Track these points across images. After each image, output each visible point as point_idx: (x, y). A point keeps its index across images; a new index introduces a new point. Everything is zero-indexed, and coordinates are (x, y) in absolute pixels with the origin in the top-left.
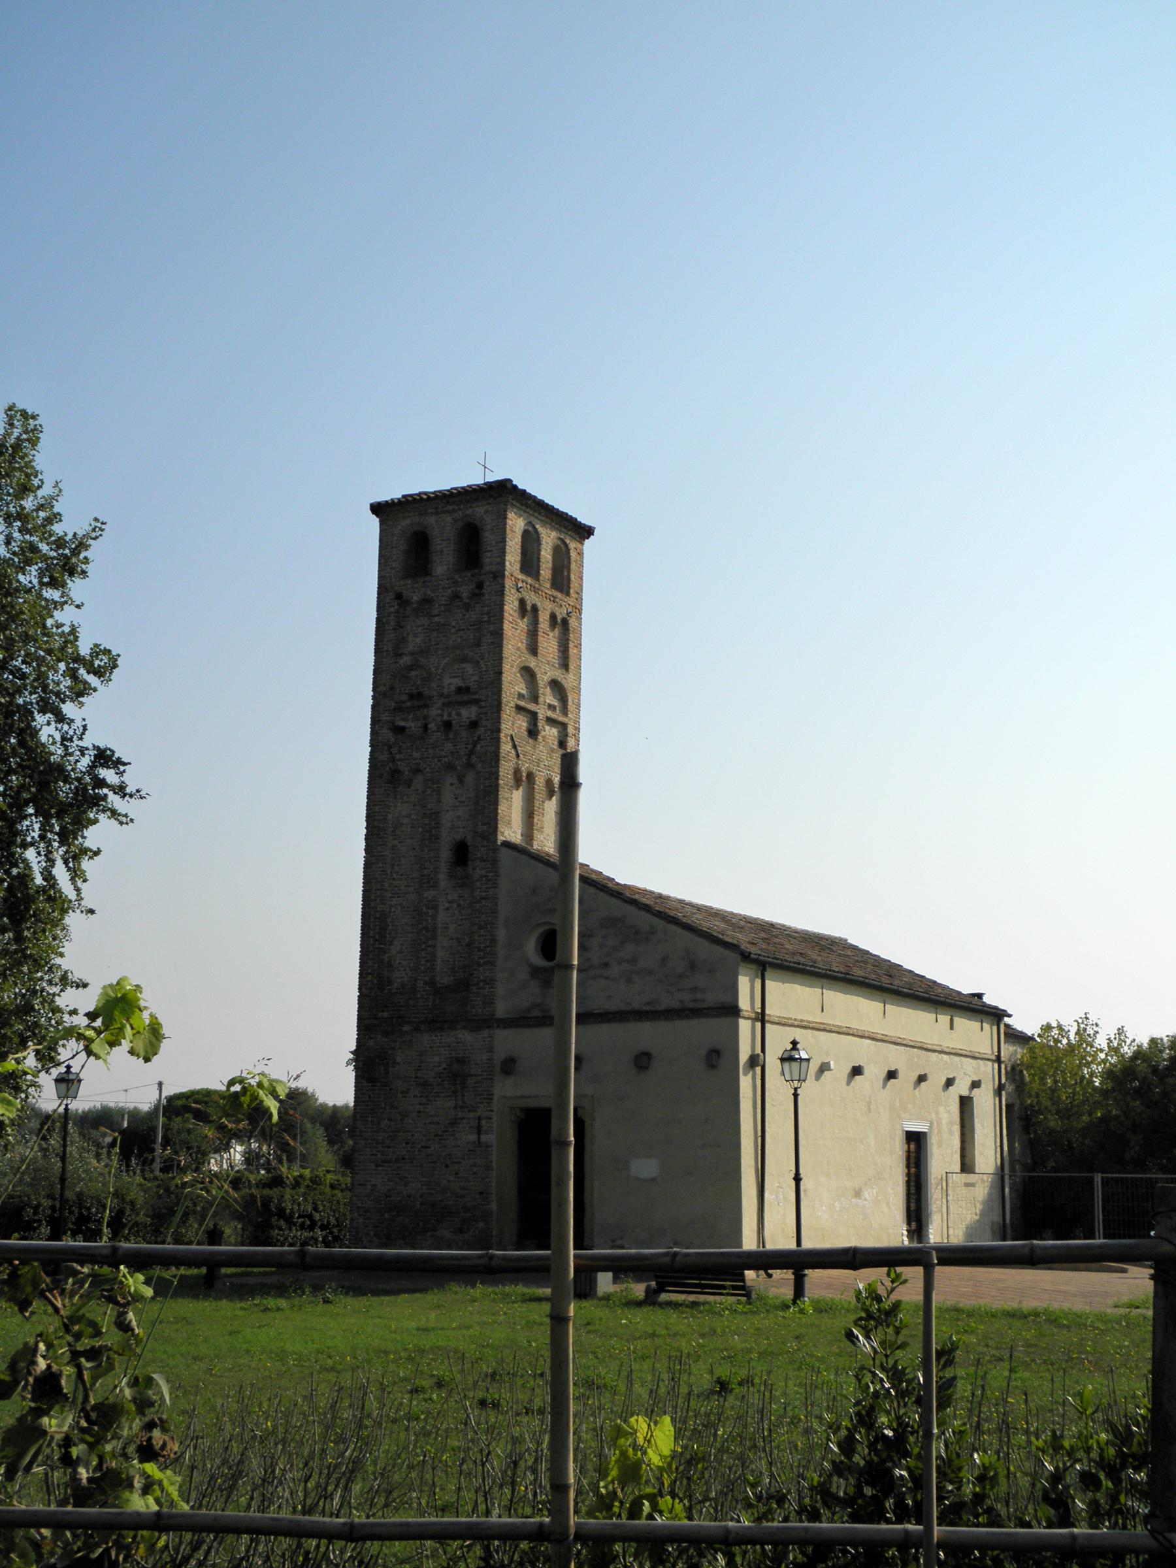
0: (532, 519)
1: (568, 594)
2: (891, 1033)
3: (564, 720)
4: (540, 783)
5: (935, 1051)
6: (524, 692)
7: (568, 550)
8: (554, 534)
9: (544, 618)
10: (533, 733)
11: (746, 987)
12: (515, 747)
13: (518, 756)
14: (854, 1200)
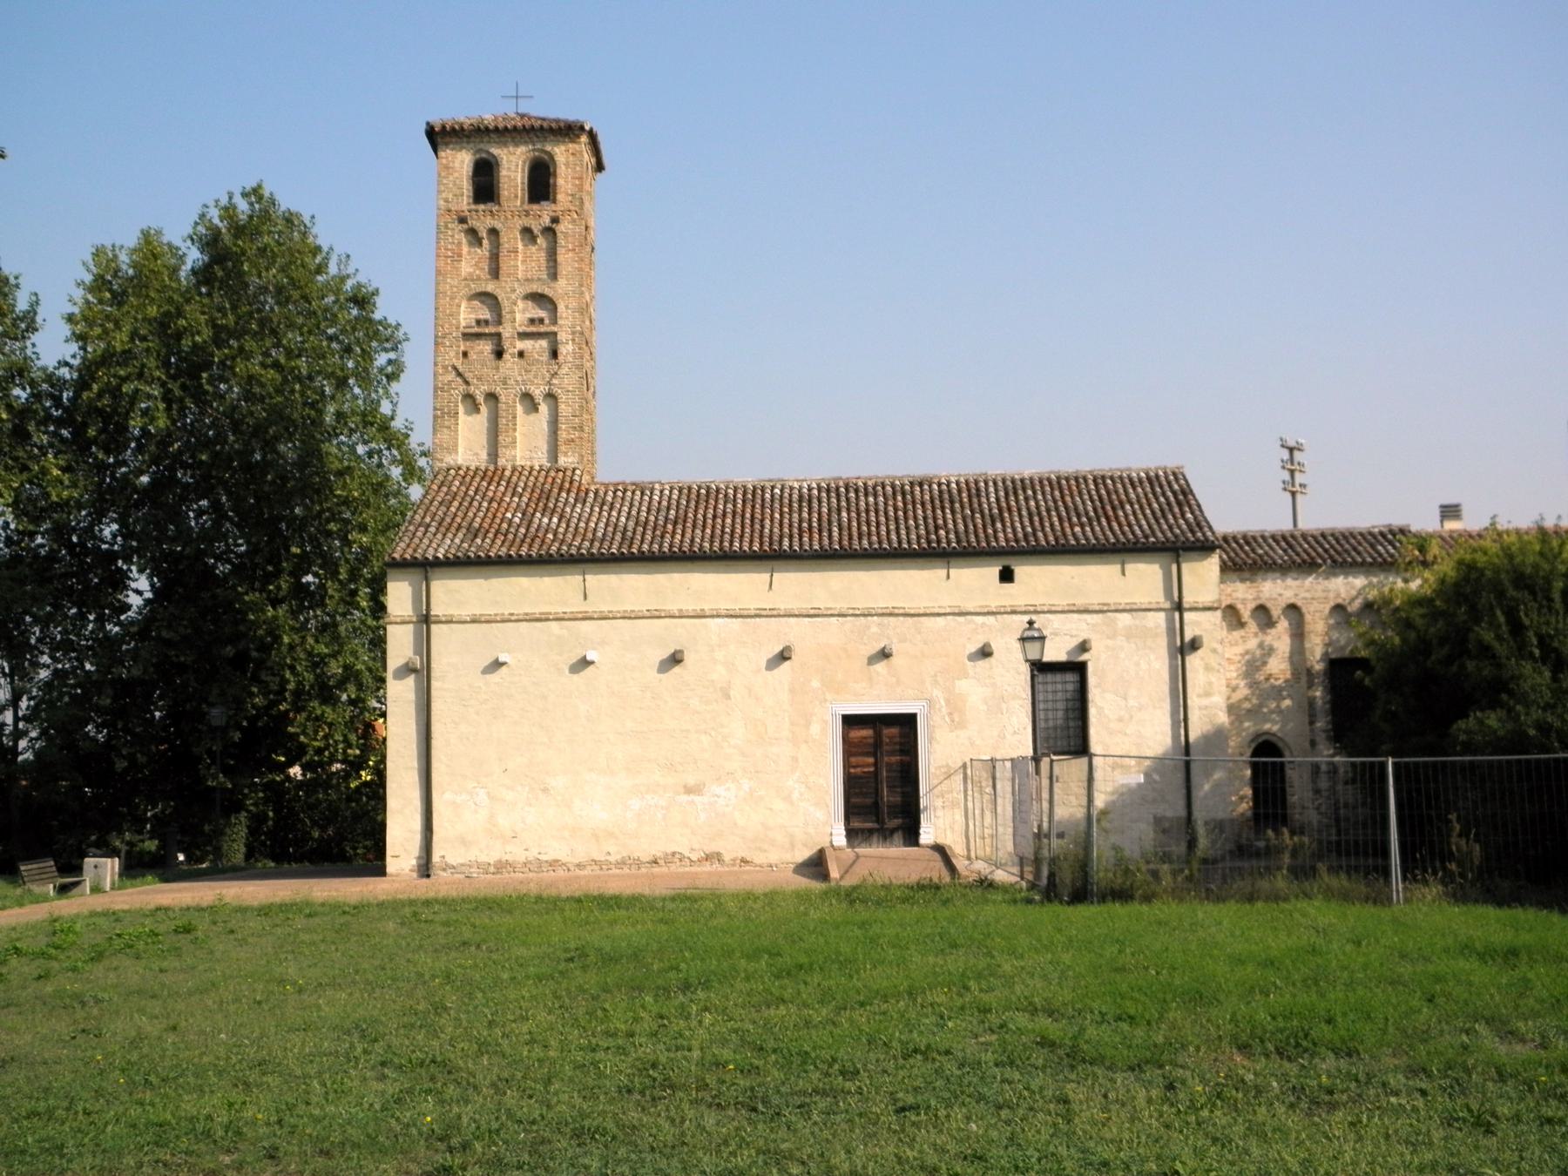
0: (481, 146)
1: (554, 201)
2: (783, 606)
3: (554, 329)
4: (507, 396)
5: (939, 615)
6: (488, 316)
7: (552, 157)
8: (522, 149)
9: (511, 238)
10: (499, 354)
11: (399, 595)
12: (459, 374)
13: (467, 383)
14: (685, 798)
